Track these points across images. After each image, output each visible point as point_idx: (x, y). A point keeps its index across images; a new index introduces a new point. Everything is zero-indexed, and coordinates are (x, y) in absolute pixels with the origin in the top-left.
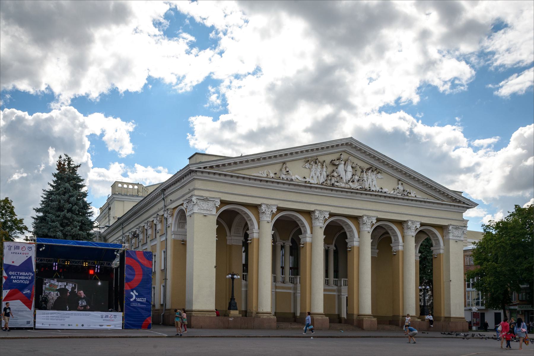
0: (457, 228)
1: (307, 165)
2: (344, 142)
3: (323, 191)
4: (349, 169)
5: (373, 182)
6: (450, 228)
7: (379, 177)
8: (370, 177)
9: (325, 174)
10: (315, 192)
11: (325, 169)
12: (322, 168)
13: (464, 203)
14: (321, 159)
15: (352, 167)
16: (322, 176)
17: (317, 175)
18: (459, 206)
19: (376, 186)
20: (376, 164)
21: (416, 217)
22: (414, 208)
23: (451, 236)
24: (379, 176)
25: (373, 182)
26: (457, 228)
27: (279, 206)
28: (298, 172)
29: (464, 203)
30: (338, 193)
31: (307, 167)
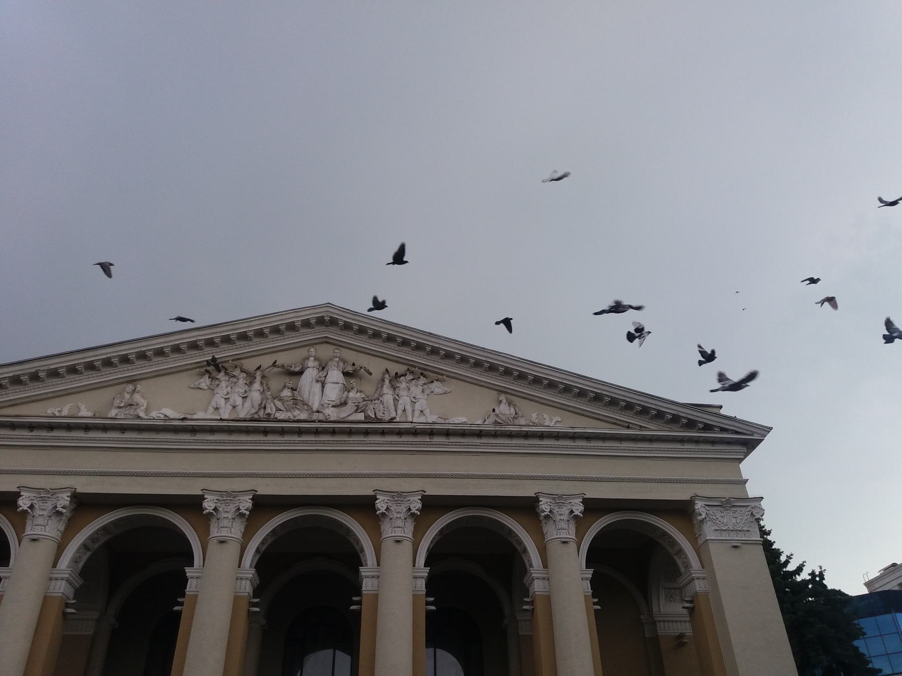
0: (726, 504)
1: (205, 382)
2: (312, 316)
3: (235, 437)
4: (335, 375)
5: (417, 404)
6: (699, 505)
7: (437, 390)
8: (403, 393)
9: (256, 395)
10: (210, 442)
11: (257, 386)
12: (251, 384)
13: (723, 430)
14: (250, 364)
15: (346, 374)
16: (248, 403)
17: (231, 400)
18: (713, 442)
19: (427, 412)
20: (419, 358)
21: (566, 482)
22: (559, 459)
23: (709, 532)
24: (437, 387)
25: (417, 404)
26: (726, 504)
27: (80, 490)
28: (167, 400)
29: (723, 430)
30: (287, 438)
31: (203, 386)
